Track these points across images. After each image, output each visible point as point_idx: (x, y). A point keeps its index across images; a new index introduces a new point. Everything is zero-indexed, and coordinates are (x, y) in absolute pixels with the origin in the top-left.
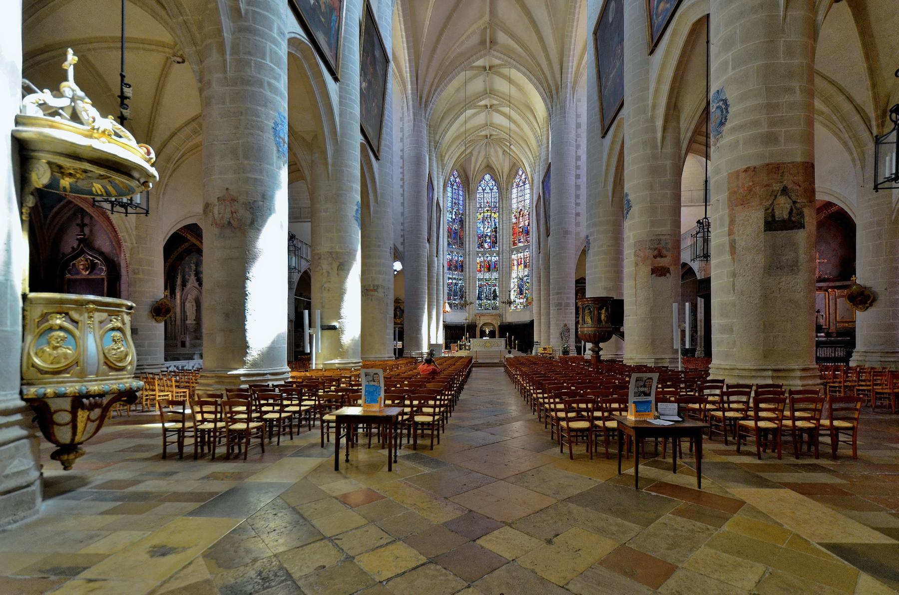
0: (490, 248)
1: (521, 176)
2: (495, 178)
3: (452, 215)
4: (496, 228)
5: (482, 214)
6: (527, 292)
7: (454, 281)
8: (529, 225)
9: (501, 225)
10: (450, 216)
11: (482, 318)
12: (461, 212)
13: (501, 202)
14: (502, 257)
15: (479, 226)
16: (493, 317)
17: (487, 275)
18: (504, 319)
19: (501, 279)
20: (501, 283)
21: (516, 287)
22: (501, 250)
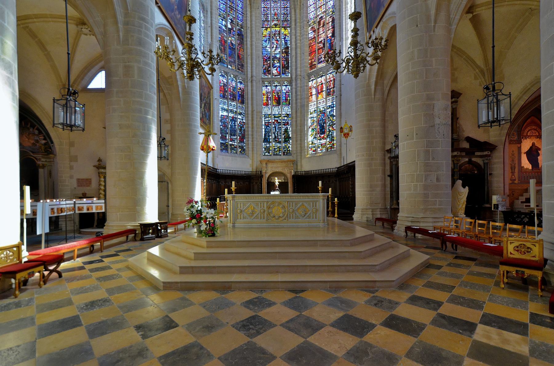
0: (279, 74)
3: (226, 21)
4: (288, 48)
5: (269, 30)
6: (331, 129)
7: (231, 115)
8: (333, 35)
9: (293, 43)
10: (224, 23)
11: (270, 165)
12: (240, 23)
13: (293, 13)
14: (296, 85)
15: (265, 44)
16: (284, 164)
17: (276, 111)
18: (299, 168)
19: (294, 115)
20: (294, 120)
21: (315, 124)
22: (294, 77)
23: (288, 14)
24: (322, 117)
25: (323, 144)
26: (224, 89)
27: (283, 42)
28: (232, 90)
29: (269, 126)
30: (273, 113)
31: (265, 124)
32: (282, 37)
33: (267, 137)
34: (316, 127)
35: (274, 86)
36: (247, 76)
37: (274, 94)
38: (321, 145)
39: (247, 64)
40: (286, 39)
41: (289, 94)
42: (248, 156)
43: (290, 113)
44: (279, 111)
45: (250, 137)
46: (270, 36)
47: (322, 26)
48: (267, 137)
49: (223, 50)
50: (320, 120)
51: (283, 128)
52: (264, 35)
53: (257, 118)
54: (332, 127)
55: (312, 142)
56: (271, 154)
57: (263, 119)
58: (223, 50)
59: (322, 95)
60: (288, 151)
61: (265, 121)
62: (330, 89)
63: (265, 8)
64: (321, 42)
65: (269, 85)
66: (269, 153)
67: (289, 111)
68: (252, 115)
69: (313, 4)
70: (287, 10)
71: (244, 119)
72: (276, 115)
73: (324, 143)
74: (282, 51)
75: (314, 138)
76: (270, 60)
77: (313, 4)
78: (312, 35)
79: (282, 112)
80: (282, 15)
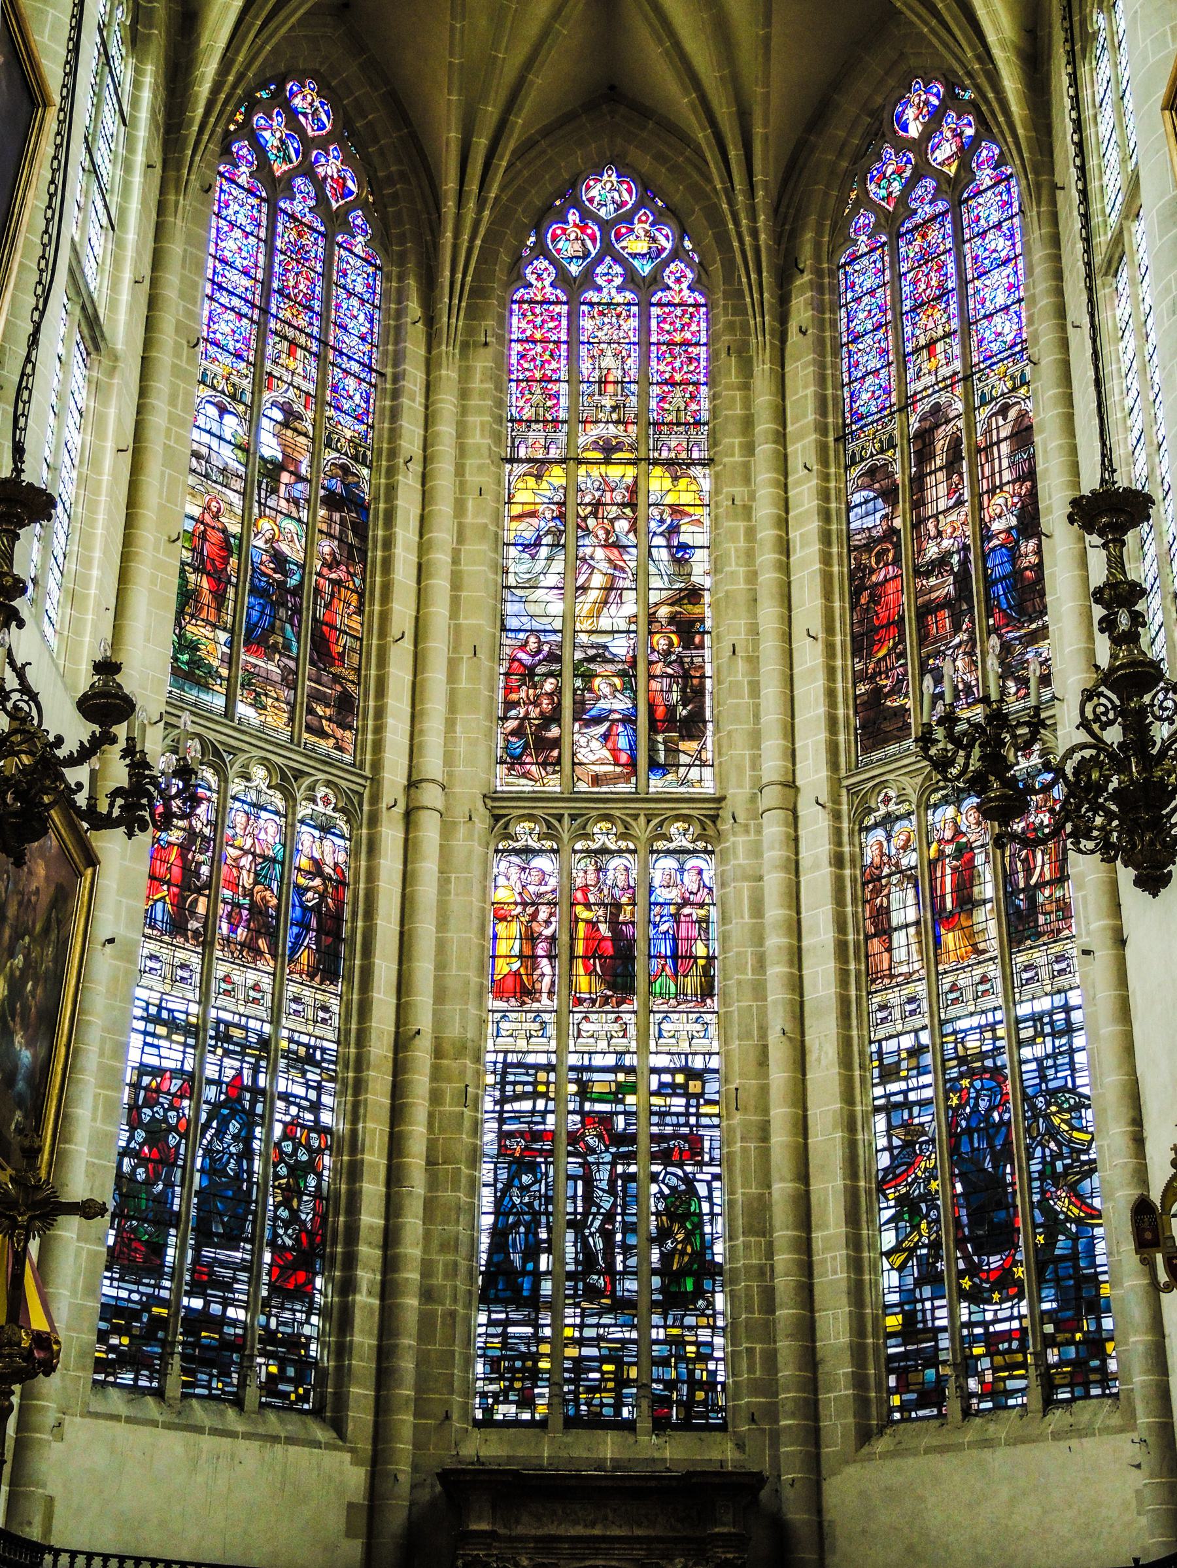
1: (921, 146)
2: (679, 195)
3: (253, 421)
5: (557, 477)
6: (1062, 1204)
9: (735, 567)
21: (931, 1159)
23: (697, 384)
24: (983, 1104)
25: (1007, 1335)
26: (185, 867)
27: (663, 555)
28: (247, 880)
29: (532, 1168)
30: (573, 1060)
31: (502, 1151)
32: (653, 525)
33: (516, 1258)
34: (934, 1185)
35: (588, 852)
36: (376, 781)
37: (585, 914)
38: (990, 1340)
39: (381, 692)
40: (684, 538)
41: (706, 920)
42: (338, 1426)
43: (714, 1063)
44: (619, 1043)
45: (369, 1252)
46: (562, 517)
47: (939, 462)
48: (516, 1258)
49: (206, 598)
50: (969, 1131)
51: (654, 1188)
52: (516, 510)
53: (435, 1097)
54: (1073, 1189)
55: (910, 1319)
56: (541, 1411)
57: (489, 1105)
58: (206, 598)
59: (970, 934)
60: (694, 1384)
61: (501, 1121)
62: (1031, 892)
63: (535, 342)
64: (943, 561)
65: (548, 844)
66: (527, 1402)
67: (700, 1044)
68: (399, 1067)
69: (877, 328)
70: (691, 360)
71: (327, 1100)
72: (596, 1076)
73: (1015, 1324)
74: (652, 619)
75: (919, 1283)
76: (557, 675)
77: (877, 328)
78: (869, 522)
79: (643, 1050)
80: (655, 390)
